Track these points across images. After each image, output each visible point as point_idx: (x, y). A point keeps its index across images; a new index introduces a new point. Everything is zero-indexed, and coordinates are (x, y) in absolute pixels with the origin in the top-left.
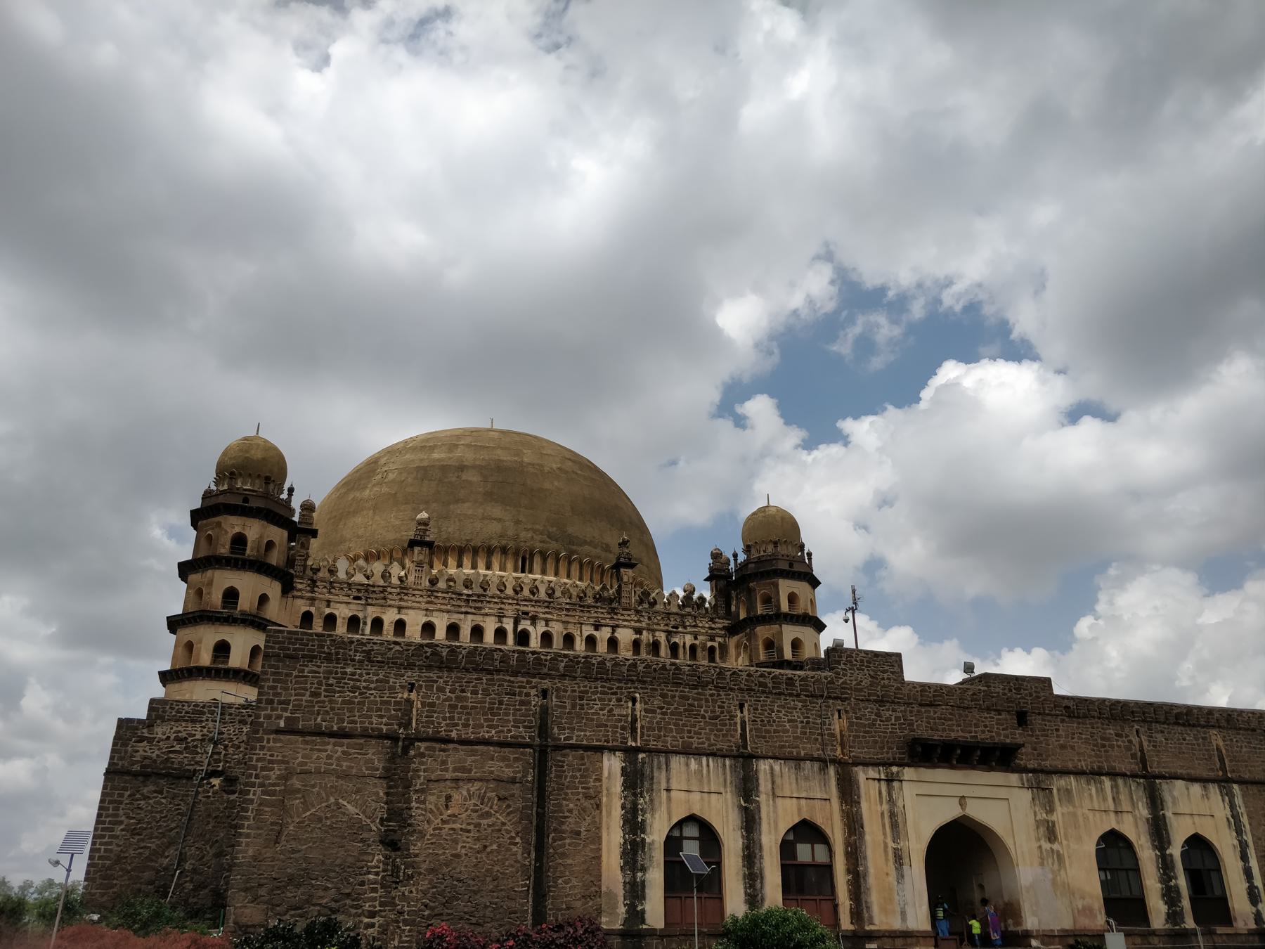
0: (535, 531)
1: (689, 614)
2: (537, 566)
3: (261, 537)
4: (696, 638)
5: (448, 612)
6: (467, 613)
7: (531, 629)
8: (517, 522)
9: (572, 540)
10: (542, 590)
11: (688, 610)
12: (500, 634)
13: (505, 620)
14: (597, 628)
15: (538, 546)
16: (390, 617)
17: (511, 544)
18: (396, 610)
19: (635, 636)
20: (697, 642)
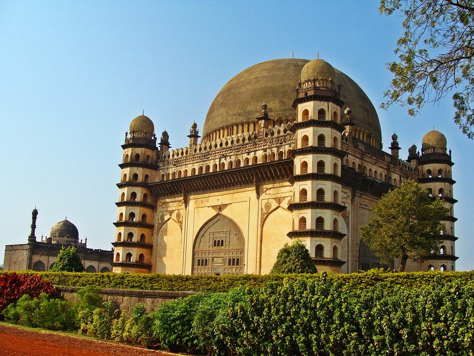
0: (233, 115)
1: (288, 134)
2: (235, 132)
3: (132, 154)
4: (290, 146)
5: (199, 162)
6: (204, 161)
7: (225, 161)
8: (228, 112)
9: (249, 113)
10: (229, 142)
11: (287, 132)
12: (215, 166)
13: (216, 160)
14: (248, 153)
15: (234, 121)
16: (183, 169)
17: (225, 124)
18: (184, 166)
19: (264, 153)
20: (291, 148)
